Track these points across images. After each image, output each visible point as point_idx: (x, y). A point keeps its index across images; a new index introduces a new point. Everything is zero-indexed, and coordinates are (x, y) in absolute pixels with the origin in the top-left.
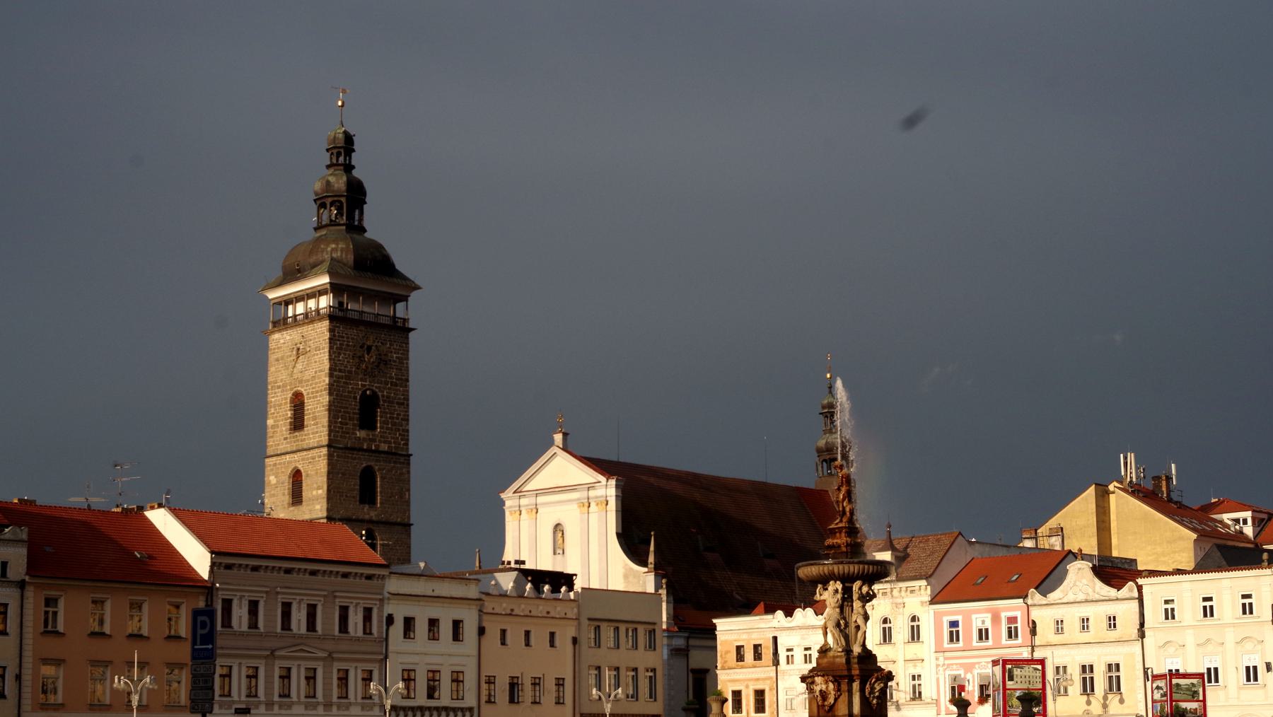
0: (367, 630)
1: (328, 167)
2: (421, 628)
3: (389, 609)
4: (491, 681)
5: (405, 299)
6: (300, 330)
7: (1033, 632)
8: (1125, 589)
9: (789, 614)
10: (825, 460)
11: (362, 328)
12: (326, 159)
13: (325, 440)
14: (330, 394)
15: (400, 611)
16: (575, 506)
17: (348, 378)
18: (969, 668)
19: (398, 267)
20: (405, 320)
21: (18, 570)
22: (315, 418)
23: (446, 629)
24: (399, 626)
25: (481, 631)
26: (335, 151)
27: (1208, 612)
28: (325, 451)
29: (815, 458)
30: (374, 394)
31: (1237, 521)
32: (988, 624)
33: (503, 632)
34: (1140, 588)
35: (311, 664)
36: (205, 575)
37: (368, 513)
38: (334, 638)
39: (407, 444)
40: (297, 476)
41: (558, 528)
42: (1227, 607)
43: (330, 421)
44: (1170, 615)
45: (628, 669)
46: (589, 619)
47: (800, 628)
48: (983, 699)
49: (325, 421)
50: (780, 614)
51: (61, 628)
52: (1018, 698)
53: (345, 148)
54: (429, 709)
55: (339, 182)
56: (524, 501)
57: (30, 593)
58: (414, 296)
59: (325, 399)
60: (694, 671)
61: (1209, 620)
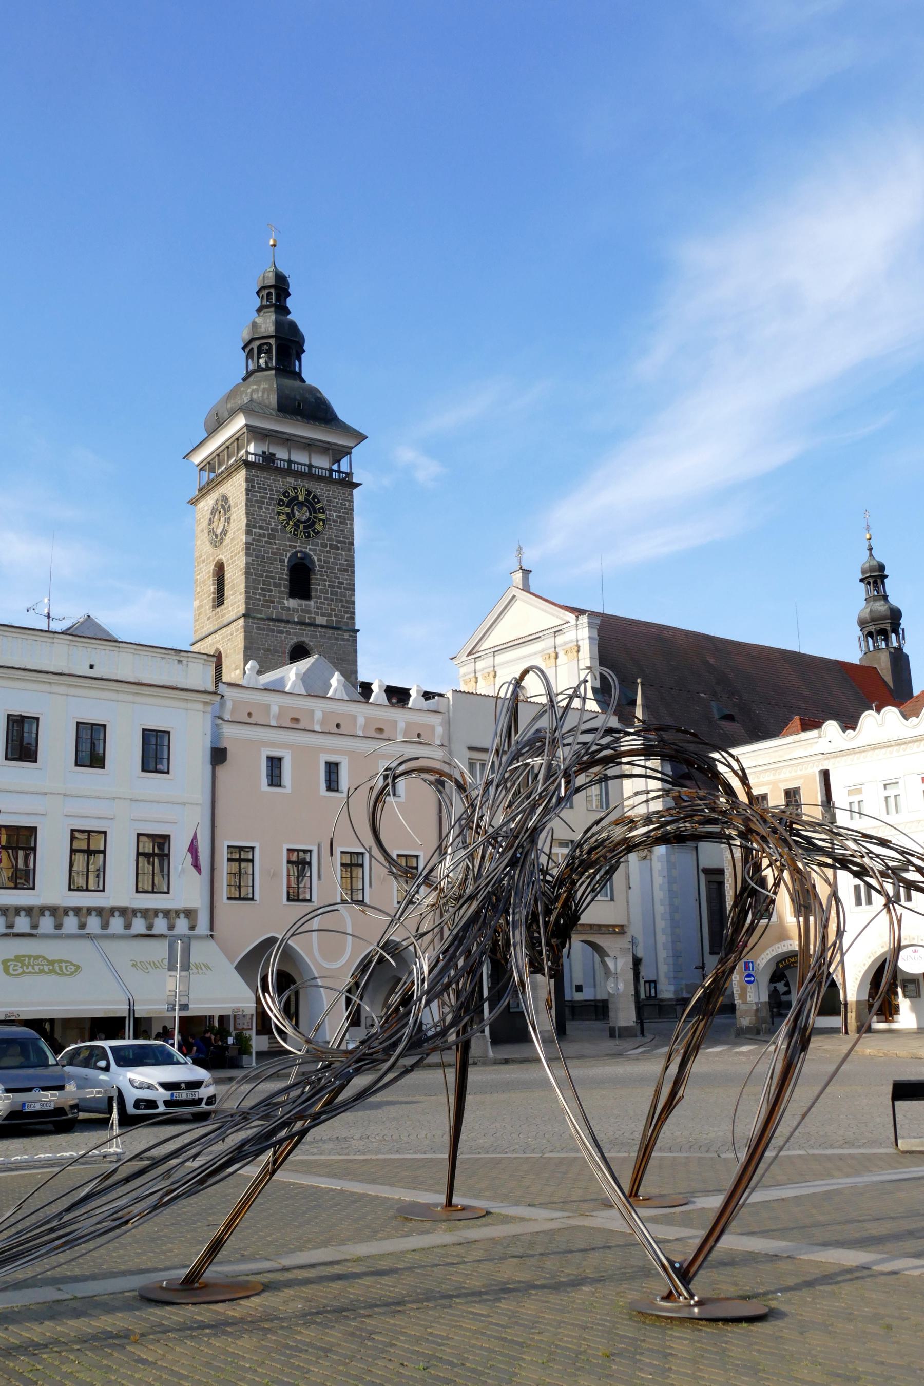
1: (259, 310)
4: (241, 856)
5: (347, 451)
9: (849, 723)
10: (870, 634)
11: (291, 480)
13: (242, 610)
14: (247, 555)
20: (349, 474)
23: (123, 748)
25: (218, 756)
26: (265, 292)
28: (241, 622)
29: (857, 631)
30: (306, 556)
33: (275, 763)
39: (353, 618)
43: (247, 587)
46: (471, 749)
47: (874, 747)
50: (831, 727)
53: (277, 292)
54: (77, 911)
55: (267, 324)
56: (480, 665)
60: (707, 871)
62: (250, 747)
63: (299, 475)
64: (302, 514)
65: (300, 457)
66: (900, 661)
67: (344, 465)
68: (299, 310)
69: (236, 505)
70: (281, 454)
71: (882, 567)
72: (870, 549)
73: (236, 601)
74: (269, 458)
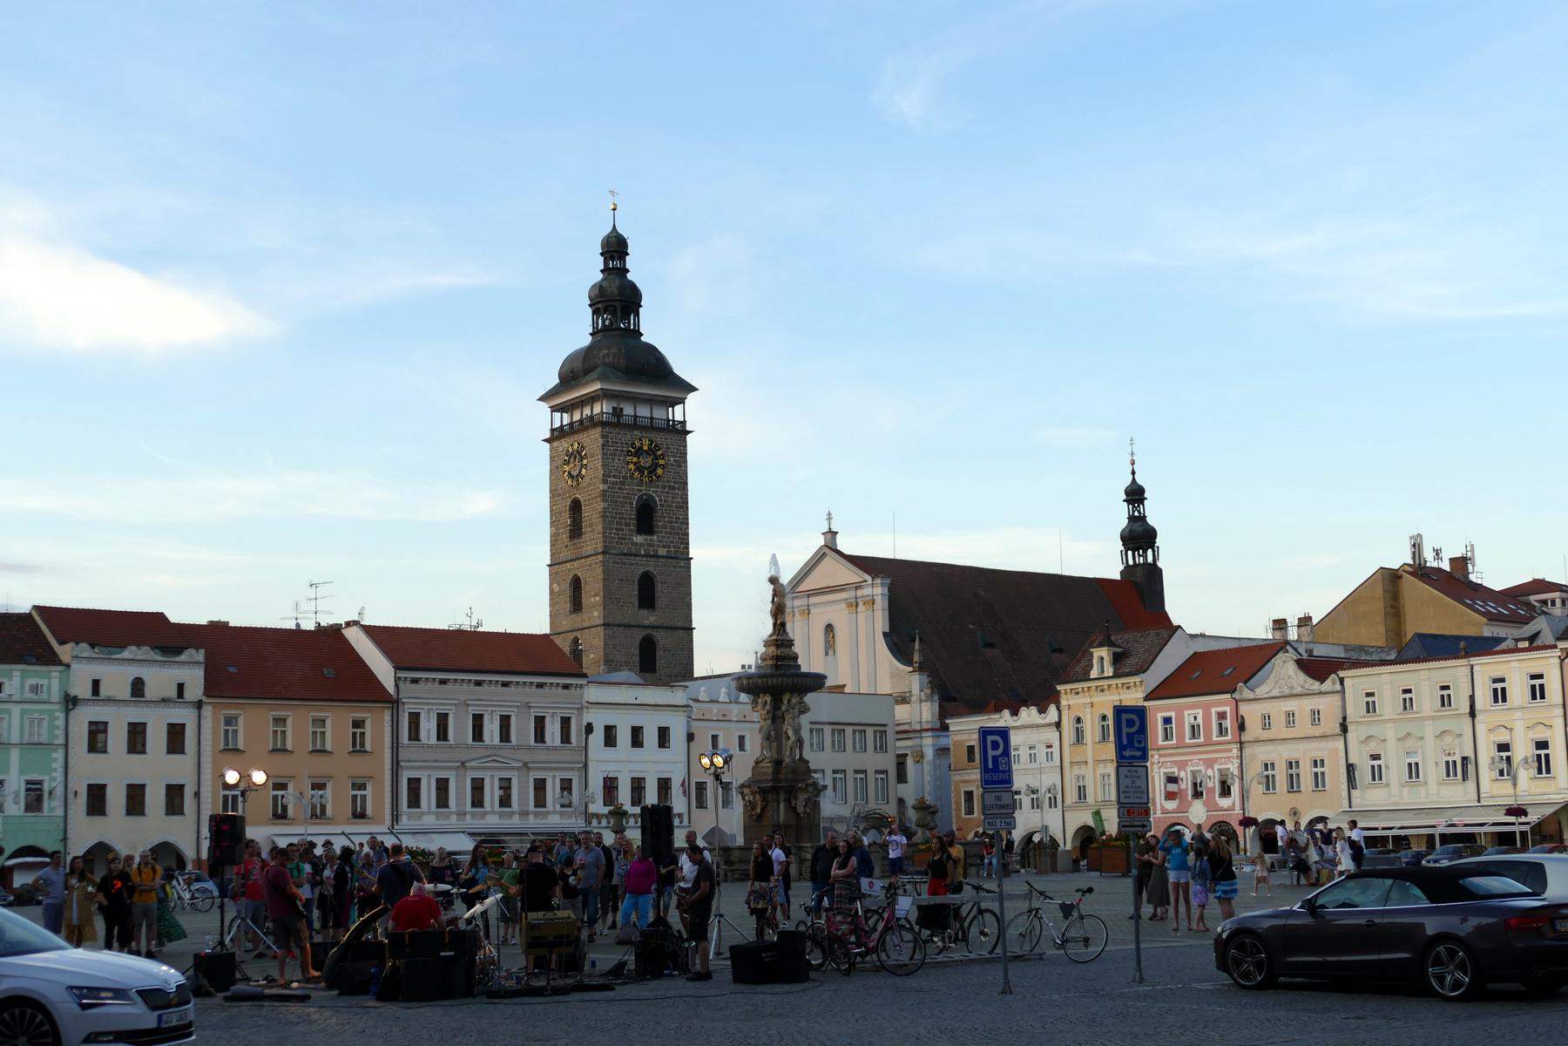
0: (566, 738)
2: (624, 737)
3: (589, 717)
5: (682, 401)
6: (576, 437)
7: (1242, 727)
8: (1328, 682)
9: (1015, 713)
11: (637, 433)
12: (600, 263)
15: (600, 719)
16: (843, 606)
17: (623, 483)
18: (1182, 765)
19: (677, 371)
20: (684, 423)
21: (195, 690)
22: (591, 525)
23: (651, 737)
24: (598, 736)
25: (690, 737)
27: (1407, 705)
31: (1544, 602)
32: (1200, 720)
34: (1342, 681)
35: (506, 775)
36: (391, 690)
37: (650, 618)
38: (530, 748)
40: (576, 584)
41: (829, 628)
42: (1427, 700)
44: (1370, 708)
45: (856, 772)
48: (1197, 794)
49: (600, 528)
50: (1006, 713)
51: (241, 746)
52: (914, 807)
57: (207, 711)
58: (691, 398)
59: (600, 505)
61: (1447, 712)
62: (703, 734)
63: (643, 428)
64: (646, 461)
65: (644, 411)
66: (1153, 575)
67: (677, 413)
68: (638, 270)
69: (592, 455)
70: (628, 410)
71: (1141, 491)
72: (1133, 473)
73: (593, 539)
74: (617, 412)
